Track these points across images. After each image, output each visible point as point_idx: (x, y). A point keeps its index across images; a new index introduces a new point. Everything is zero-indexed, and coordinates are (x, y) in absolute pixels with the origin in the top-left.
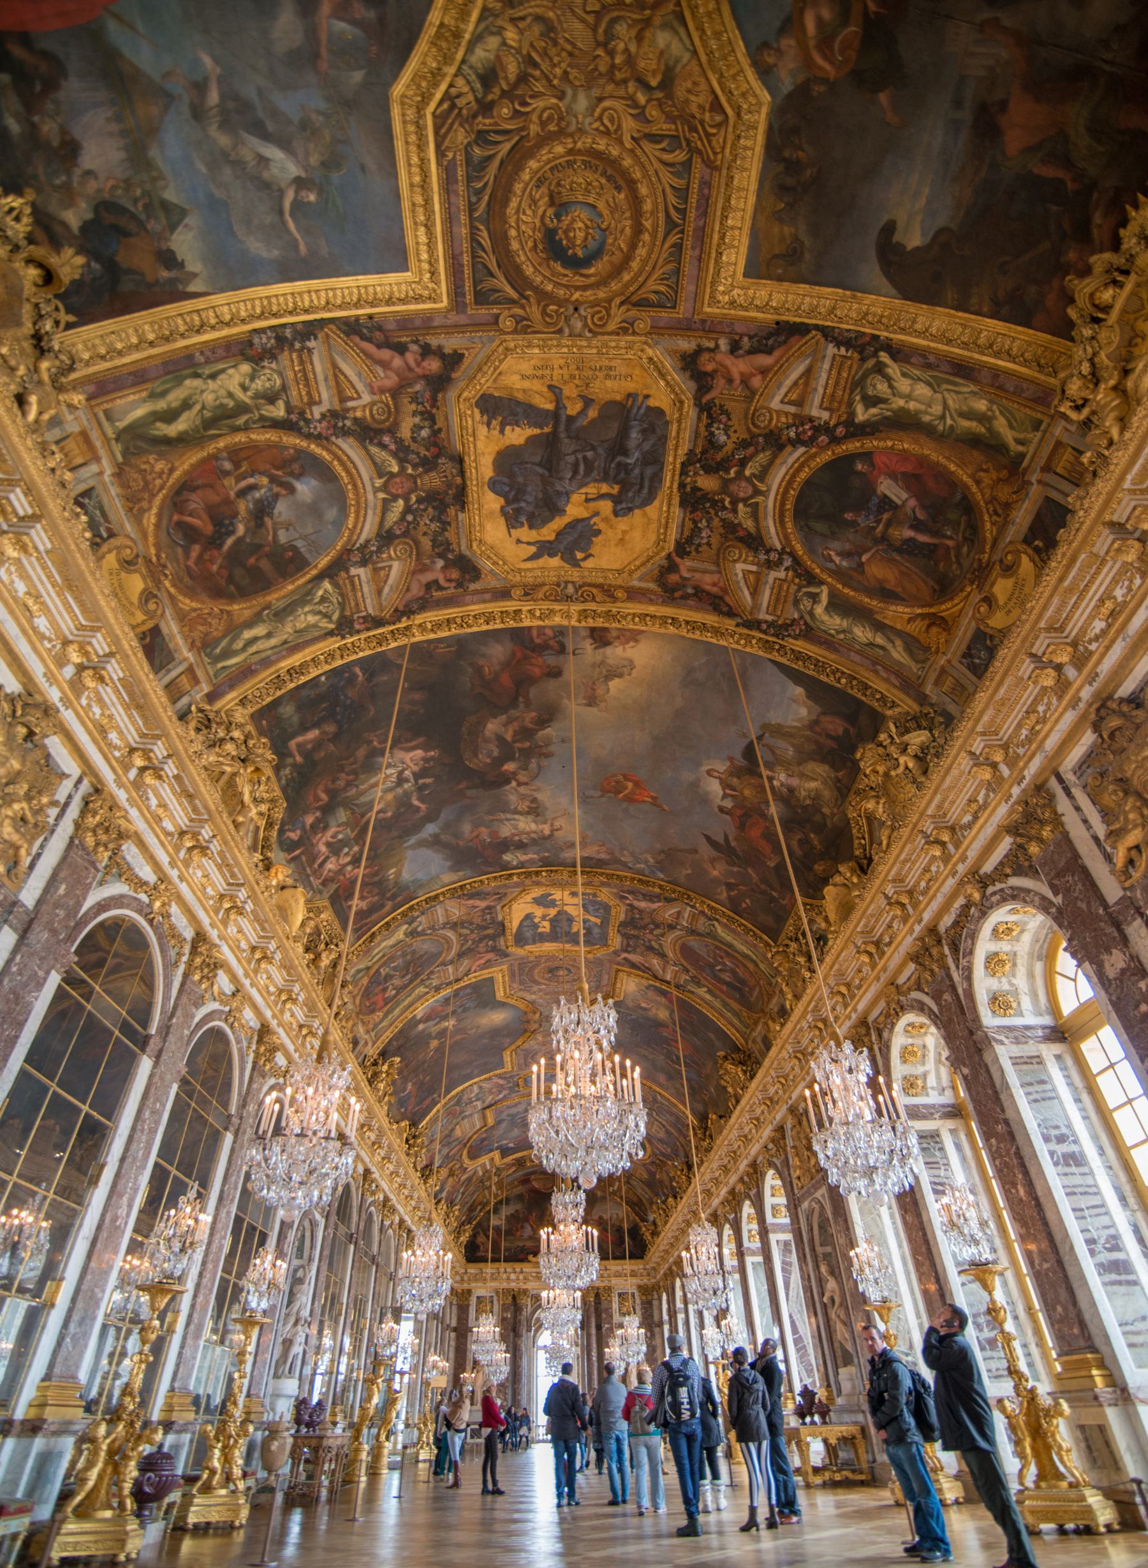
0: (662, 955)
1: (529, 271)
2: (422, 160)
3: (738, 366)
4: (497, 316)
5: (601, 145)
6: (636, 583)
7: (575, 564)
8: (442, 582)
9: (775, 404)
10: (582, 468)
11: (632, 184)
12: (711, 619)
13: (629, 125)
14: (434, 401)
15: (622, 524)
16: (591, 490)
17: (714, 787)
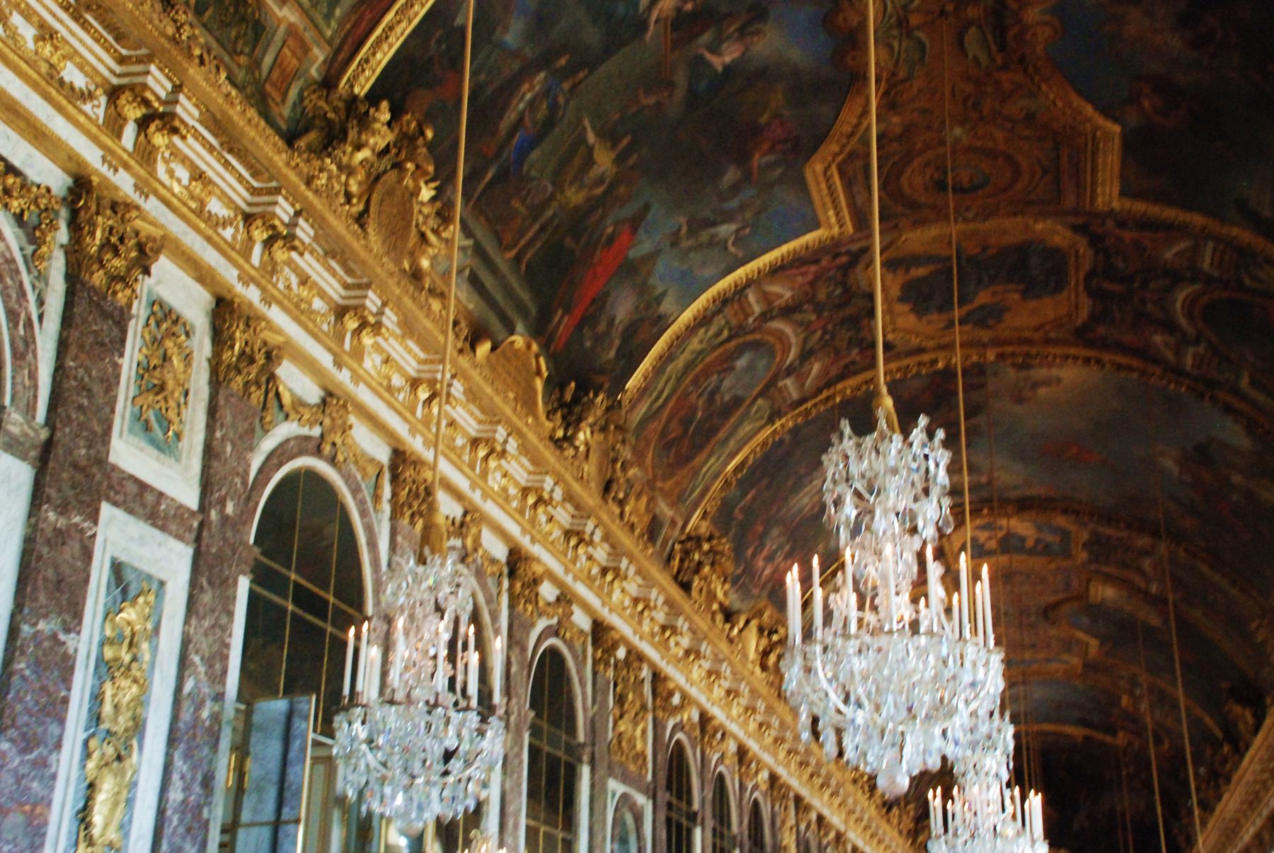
0: (1141, 572)
1: (923, 199)
2: (829, 187)
3: (1127, 235)
4: (896, 226)
5: (979, 144)
6: (1052, 335)
7: (988, 327)
8: (858, 359)
9: (1168, 255)
10: (986, 279)
11: (1009, 159)
12: (1135, 363)
13: (999, 135)
14: (845, 275)
15: (1032, 304)
16: (999, 288)
17: (1169, 464)
